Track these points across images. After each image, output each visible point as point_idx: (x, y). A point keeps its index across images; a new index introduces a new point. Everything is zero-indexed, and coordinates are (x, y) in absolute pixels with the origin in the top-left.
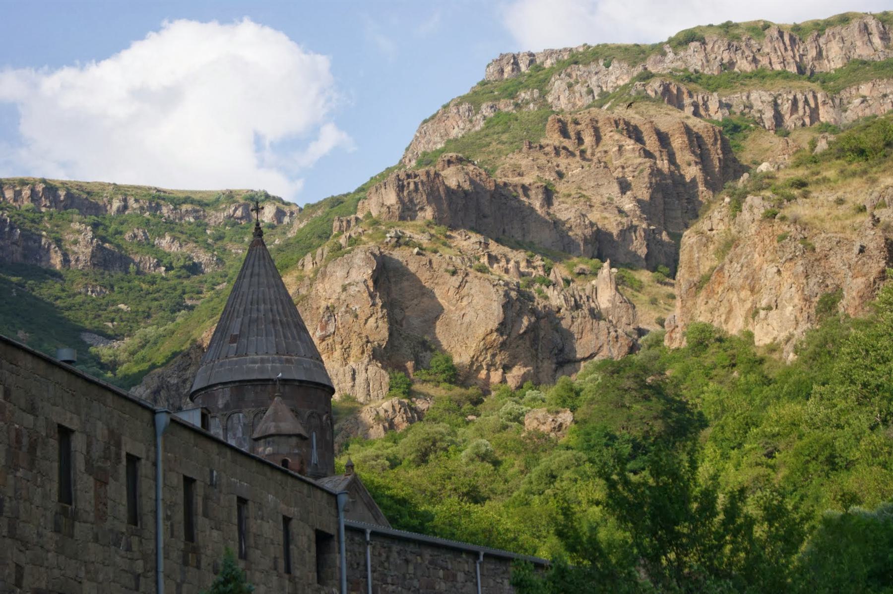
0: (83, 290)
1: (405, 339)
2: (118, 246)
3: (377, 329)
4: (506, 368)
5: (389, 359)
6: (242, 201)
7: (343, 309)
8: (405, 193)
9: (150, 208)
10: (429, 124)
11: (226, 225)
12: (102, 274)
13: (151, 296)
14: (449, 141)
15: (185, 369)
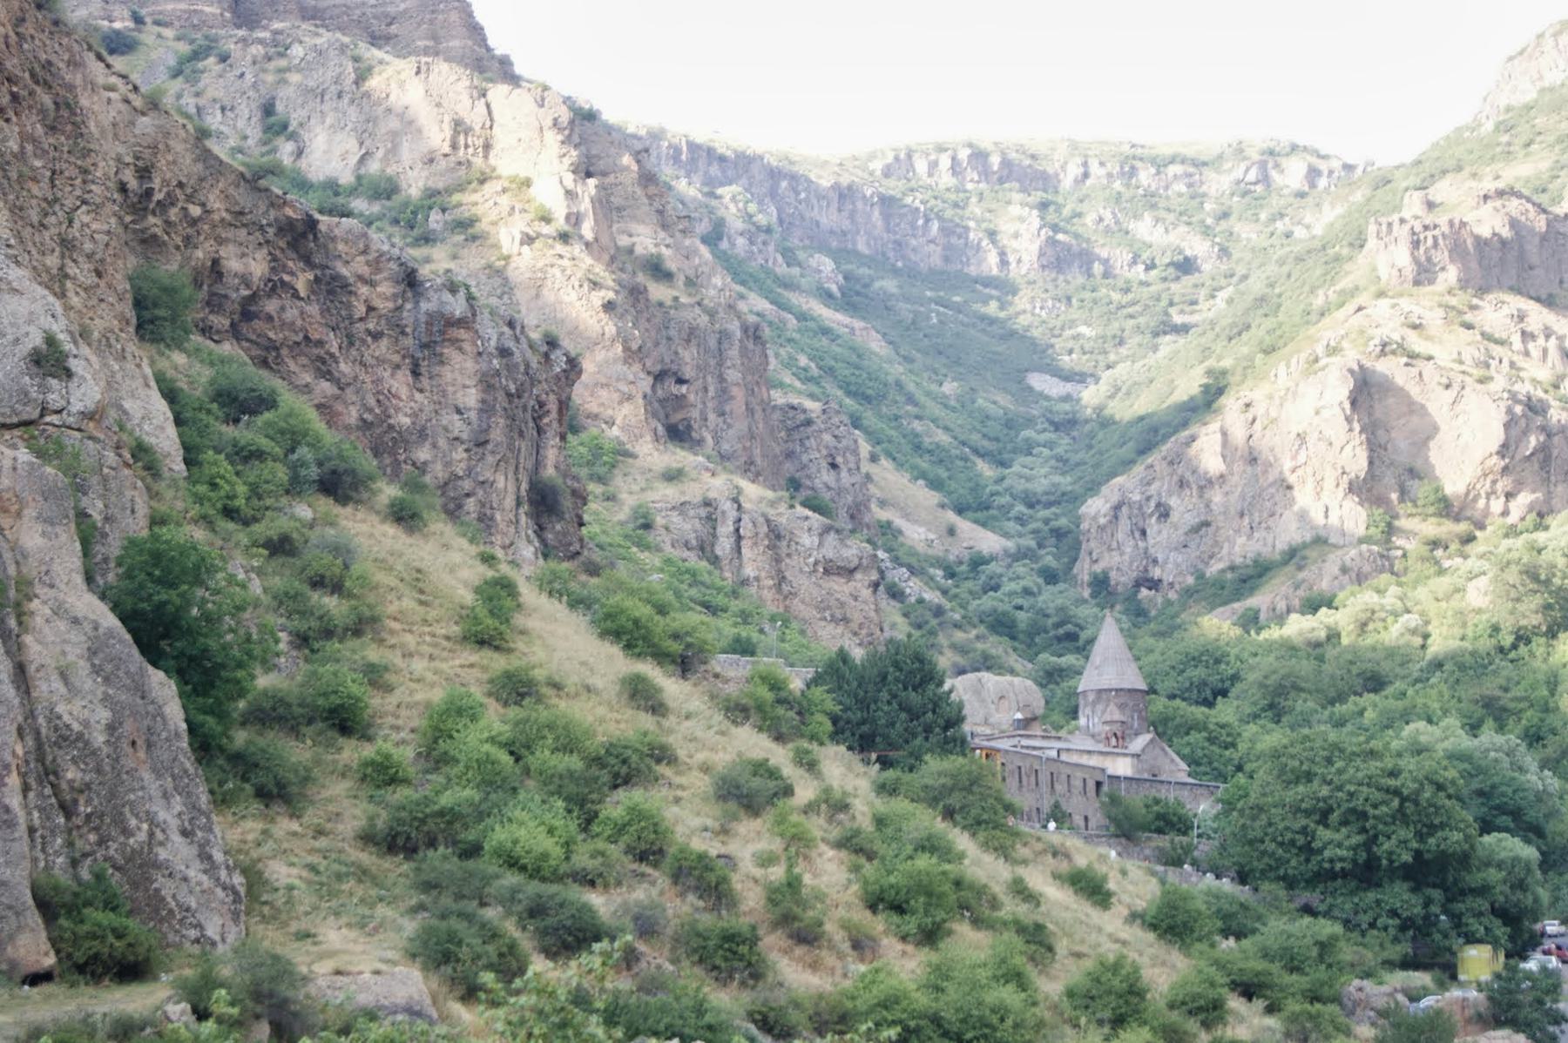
0: (1028, 307)
1: (1388, 467)
2: (1077, 236)
3: (1356, 460)
4: (1509, 496)
5: (1369, 490)
6: (1256, 157)
7: (1316, 435)
8: (1422, 249)
9: (1123, 173)
10: (1516, 62)
11: (1233, 194)
12: (1055, 280)
13: (1125, 311)
14: (1543, 90)
15: (1149, 484)
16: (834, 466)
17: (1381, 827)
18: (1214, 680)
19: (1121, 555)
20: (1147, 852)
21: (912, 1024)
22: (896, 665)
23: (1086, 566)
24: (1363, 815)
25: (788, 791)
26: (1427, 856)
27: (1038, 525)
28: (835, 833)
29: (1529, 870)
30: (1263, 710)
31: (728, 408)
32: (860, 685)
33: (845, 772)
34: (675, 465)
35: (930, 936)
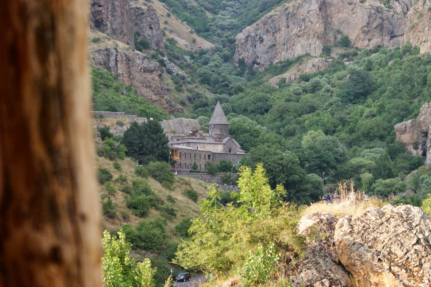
4: (369, 40)
15: (257, 30)
16: (151, 28)
17: (277, 174)
18: (265, 106)
19: (249, 52)
20: (218, 178)
21: (134, 238)
22: (150, 127)
23: (237, 56)
24: (272, 171)
25: (111, 177)
26: (289, 181)
27: (224, 39)
28: (123, 187)
29: (320, 184)
30: (278, 118)
31: (115, 14)
32: (139, 133)
33: (129, 167)
34: (97, 37)
35: (143, 215)
